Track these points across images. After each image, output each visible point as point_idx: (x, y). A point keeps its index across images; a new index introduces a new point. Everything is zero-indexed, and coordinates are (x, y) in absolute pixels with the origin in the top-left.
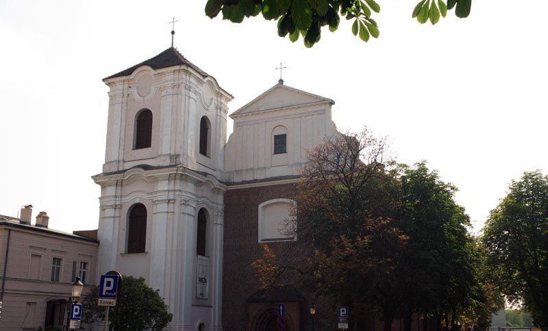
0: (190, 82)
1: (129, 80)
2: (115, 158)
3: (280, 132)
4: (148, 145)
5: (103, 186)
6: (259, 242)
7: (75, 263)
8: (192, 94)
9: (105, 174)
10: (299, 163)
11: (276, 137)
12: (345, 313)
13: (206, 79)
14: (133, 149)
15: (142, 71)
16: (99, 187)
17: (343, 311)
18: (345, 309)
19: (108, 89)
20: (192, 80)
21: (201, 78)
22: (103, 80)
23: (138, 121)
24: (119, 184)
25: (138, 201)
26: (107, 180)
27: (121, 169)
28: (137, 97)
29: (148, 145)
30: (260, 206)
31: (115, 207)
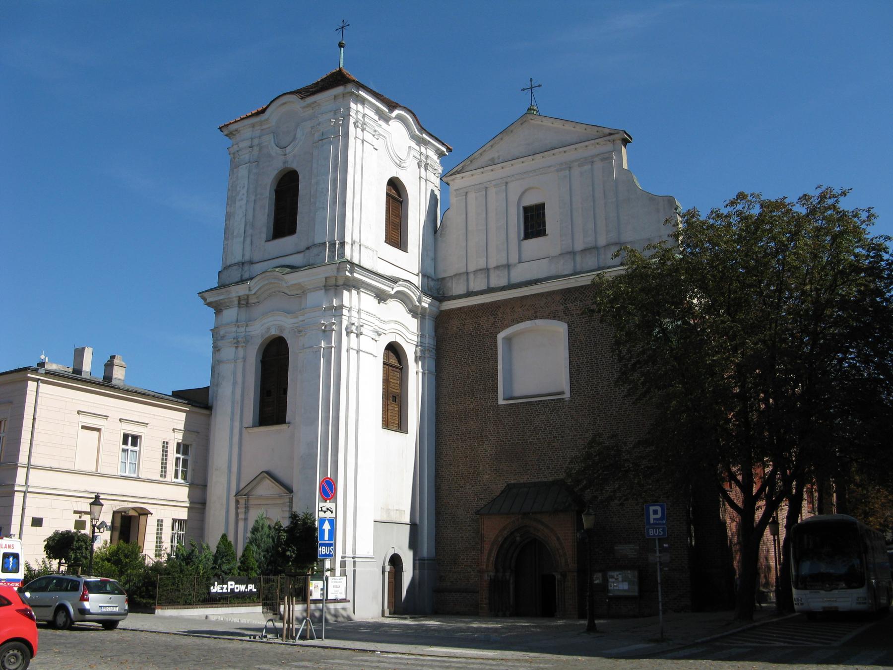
0: (364, 115)
1: (261, 123)
2: (237, 256)
3: (531, 200)
4: (292, 231)
5: (218, 308)
6: (501, 402)
7: (165, 445)
8: (368, 136)
9: (222, 286)
10: (569, 253)
11: (526, 210)
12: (659, 516)
13: (396, 112)
14: (267, 241)
15: (284, 104)
16: (212, 311)
17: (655, 512)
18: (659, 508)
19: (228, 142)
20: (371, 113)
21: (386, 110)
22: (220, 128)
23: (276, 191)
24: (244, 303)
25: (274, 332)
26: (222, 297)
27: (246, 276)
28: (274, 150)
29: (292, 231)
30: (501, 336)
31: (237, 344)
